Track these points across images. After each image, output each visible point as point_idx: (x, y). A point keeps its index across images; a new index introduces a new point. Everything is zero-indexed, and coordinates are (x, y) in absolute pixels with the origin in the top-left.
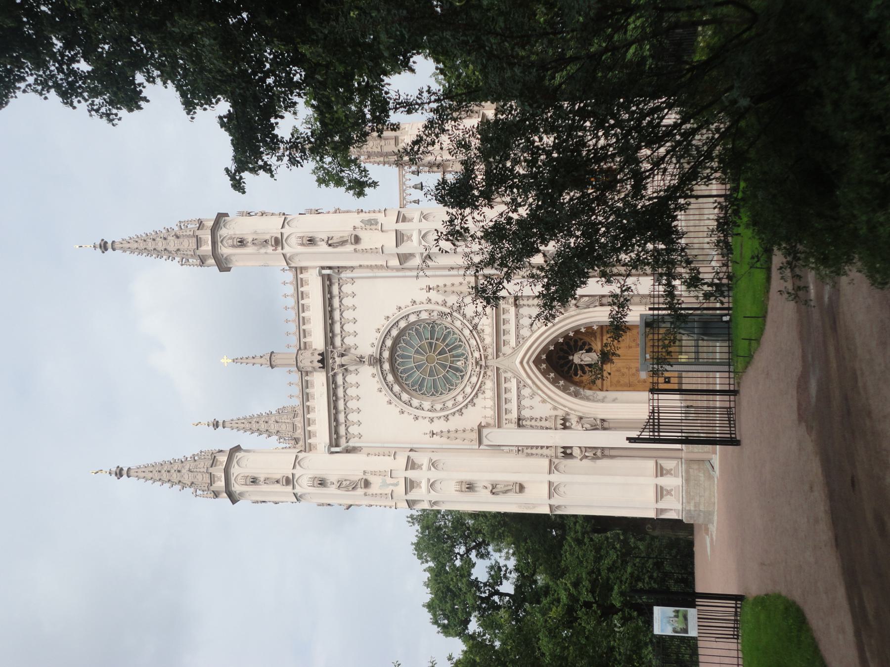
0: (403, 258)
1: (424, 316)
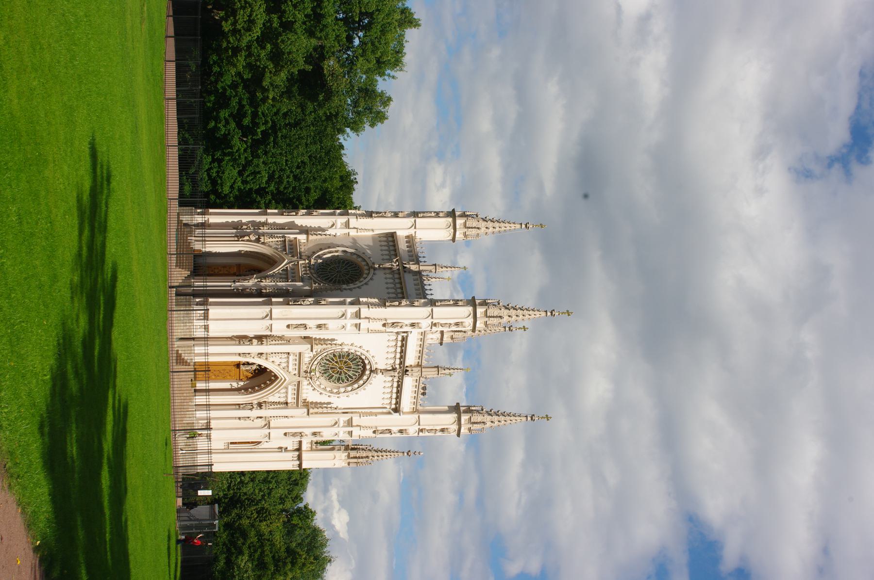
0: (350, 423)
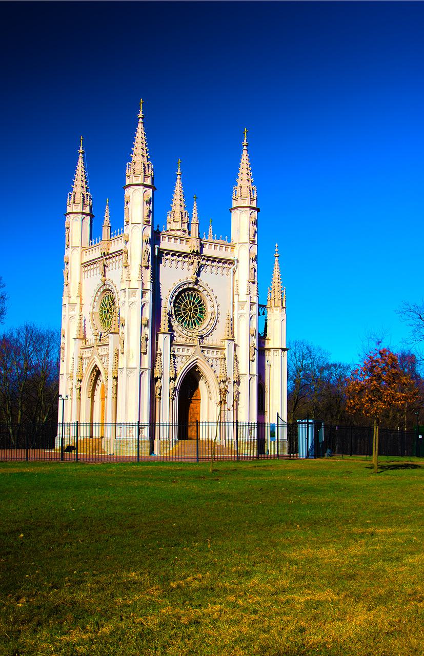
0: (242, 303)
1: (209, 310)
